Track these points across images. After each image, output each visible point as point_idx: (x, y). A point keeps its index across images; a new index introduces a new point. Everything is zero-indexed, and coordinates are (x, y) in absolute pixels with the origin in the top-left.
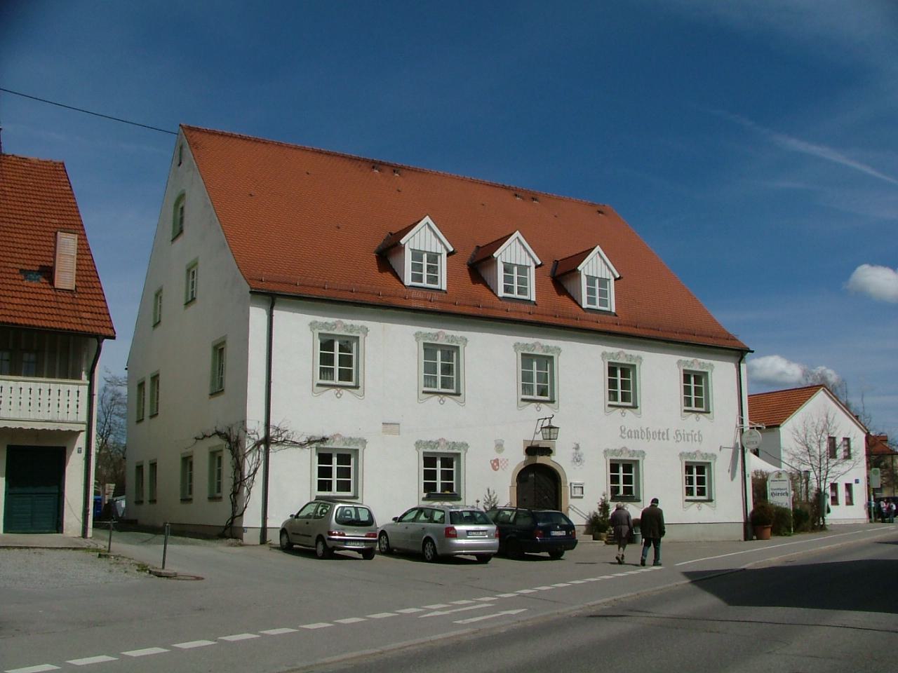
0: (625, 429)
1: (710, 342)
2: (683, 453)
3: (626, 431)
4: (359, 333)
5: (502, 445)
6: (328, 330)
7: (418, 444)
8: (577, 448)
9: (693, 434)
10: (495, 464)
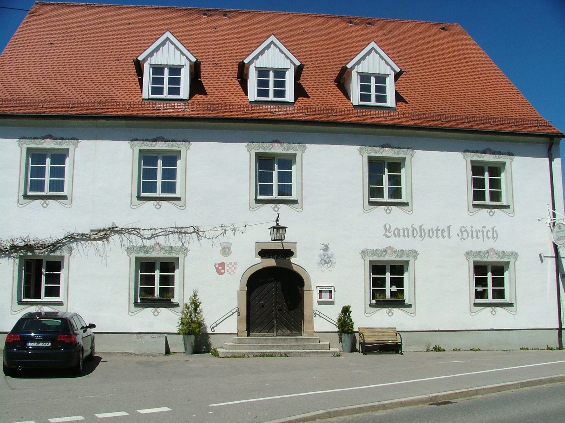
0: (390, 227)
1: (513, 129)
2: (471, 251)
3: (392, 229)
4: (69, 145)
5: (229, 248)
6: (37, 145)
7: (468, 254)
8: (326, 248)
9: (485, 230)
10: (220, 268)
